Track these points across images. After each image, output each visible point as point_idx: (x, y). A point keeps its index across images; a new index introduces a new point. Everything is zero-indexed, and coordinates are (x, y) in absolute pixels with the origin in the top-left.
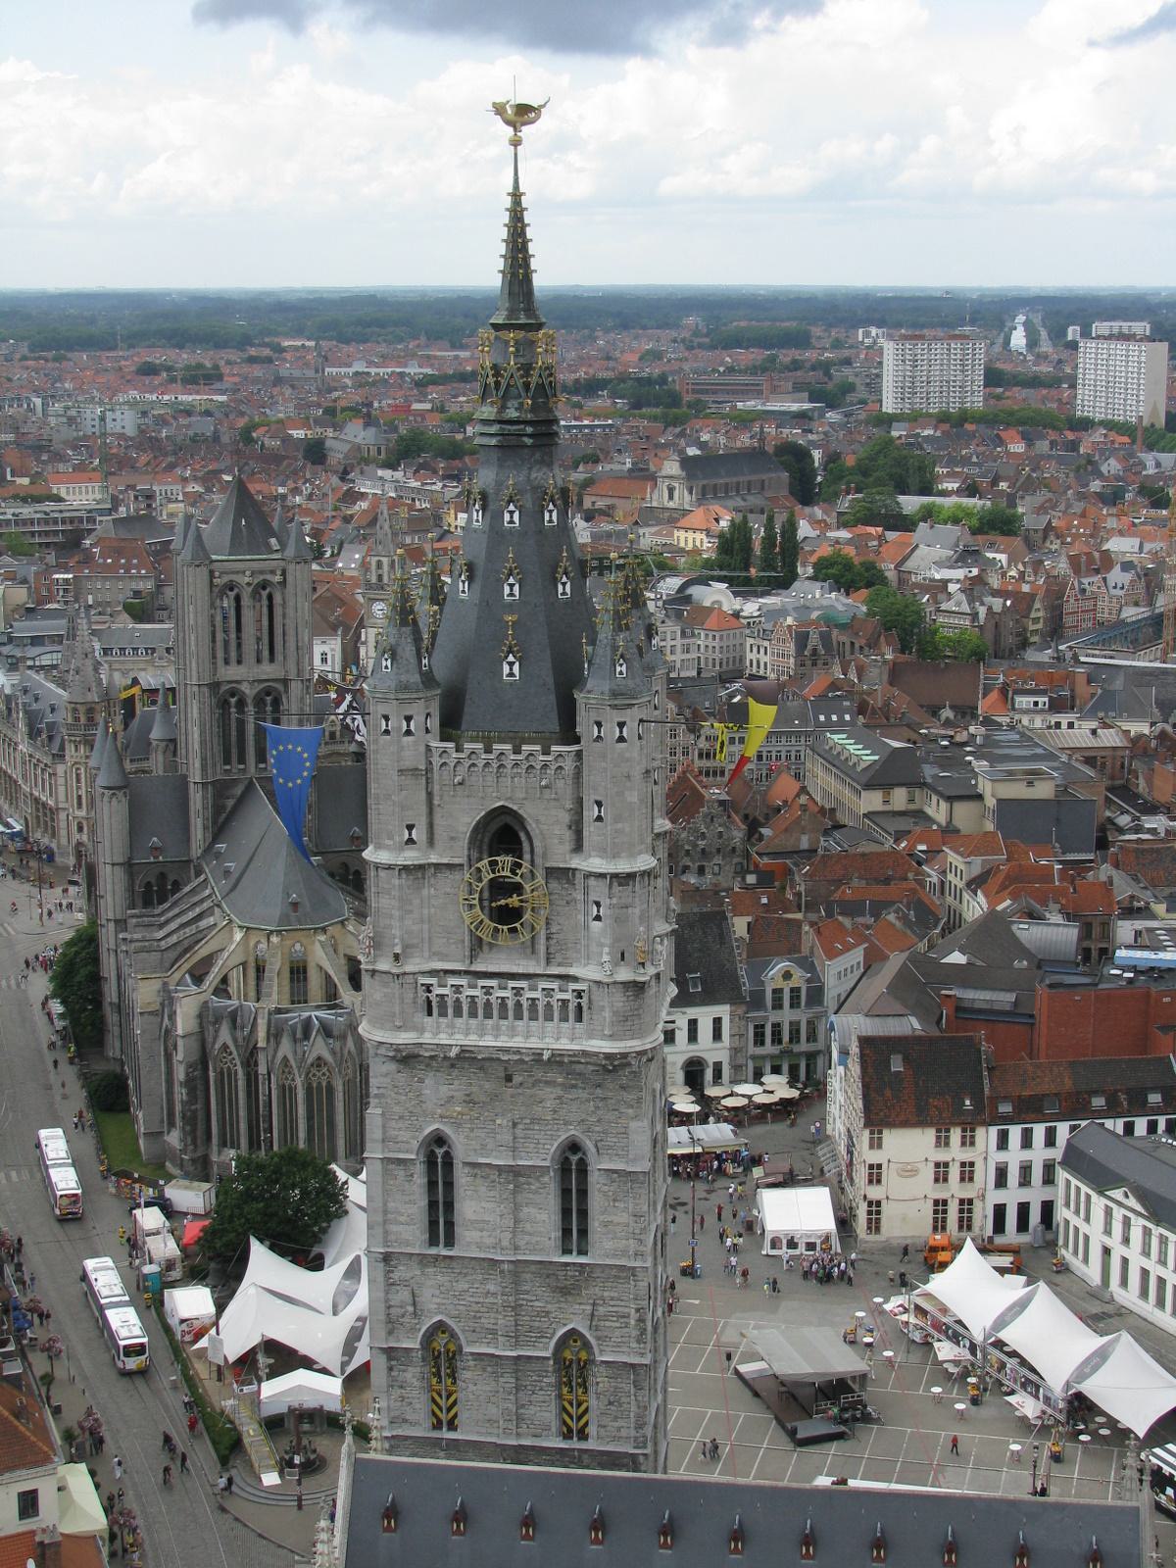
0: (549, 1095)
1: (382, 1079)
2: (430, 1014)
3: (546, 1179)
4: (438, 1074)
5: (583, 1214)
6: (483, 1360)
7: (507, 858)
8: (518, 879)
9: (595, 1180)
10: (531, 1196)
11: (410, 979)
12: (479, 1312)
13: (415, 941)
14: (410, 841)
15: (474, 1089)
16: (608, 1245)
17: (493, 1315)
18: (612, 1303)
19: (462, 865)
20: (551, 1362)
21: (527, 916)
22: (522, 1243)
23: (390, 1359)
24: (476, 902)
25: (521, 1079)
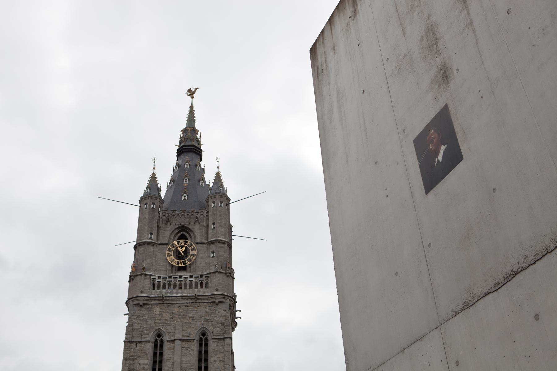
2: (154, 289)
7: (183, 240)
11: (148, 277)
19: (167, 244)
21: (190, 257)
24: (172, 254)
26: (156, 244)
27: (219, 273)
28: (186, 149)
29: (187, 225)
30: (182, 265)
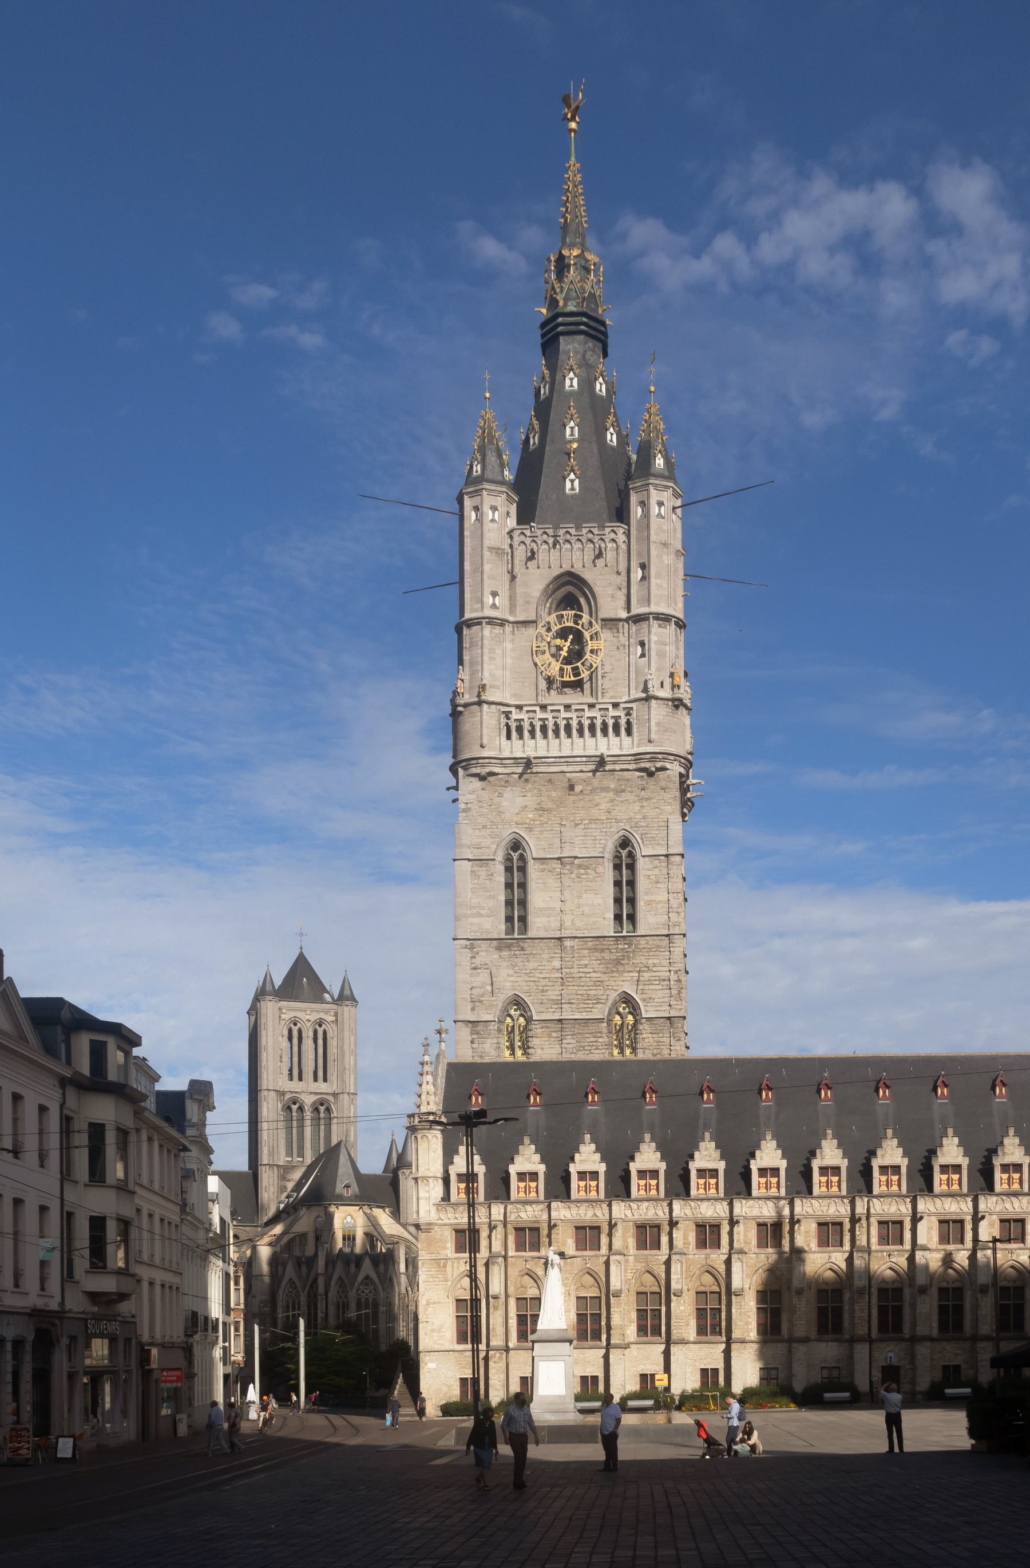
0: (603, 800)
1: (469, 796)
2: (509, 737)
3: (600, 869)
4: (515, 788)
5: (632, 901)
6: (548, 1027)
8: (580, 627)
9: (642, 864)
10: (589, 884)
12: (547, 986)
13: (497, 683)
14: (494, 606)
15: (543, 799)
16: (652, 920)
17: (557, 988)
18: (654, 969)
20: (605, 1024)
21: (588, 656)
22: (579, 923)
23: (472, 1034)
25: (581, 787)
26: (508, 621)
27: (657, 698)
28: (561, 324)
29: (578, 569)
30: (570, 677)
